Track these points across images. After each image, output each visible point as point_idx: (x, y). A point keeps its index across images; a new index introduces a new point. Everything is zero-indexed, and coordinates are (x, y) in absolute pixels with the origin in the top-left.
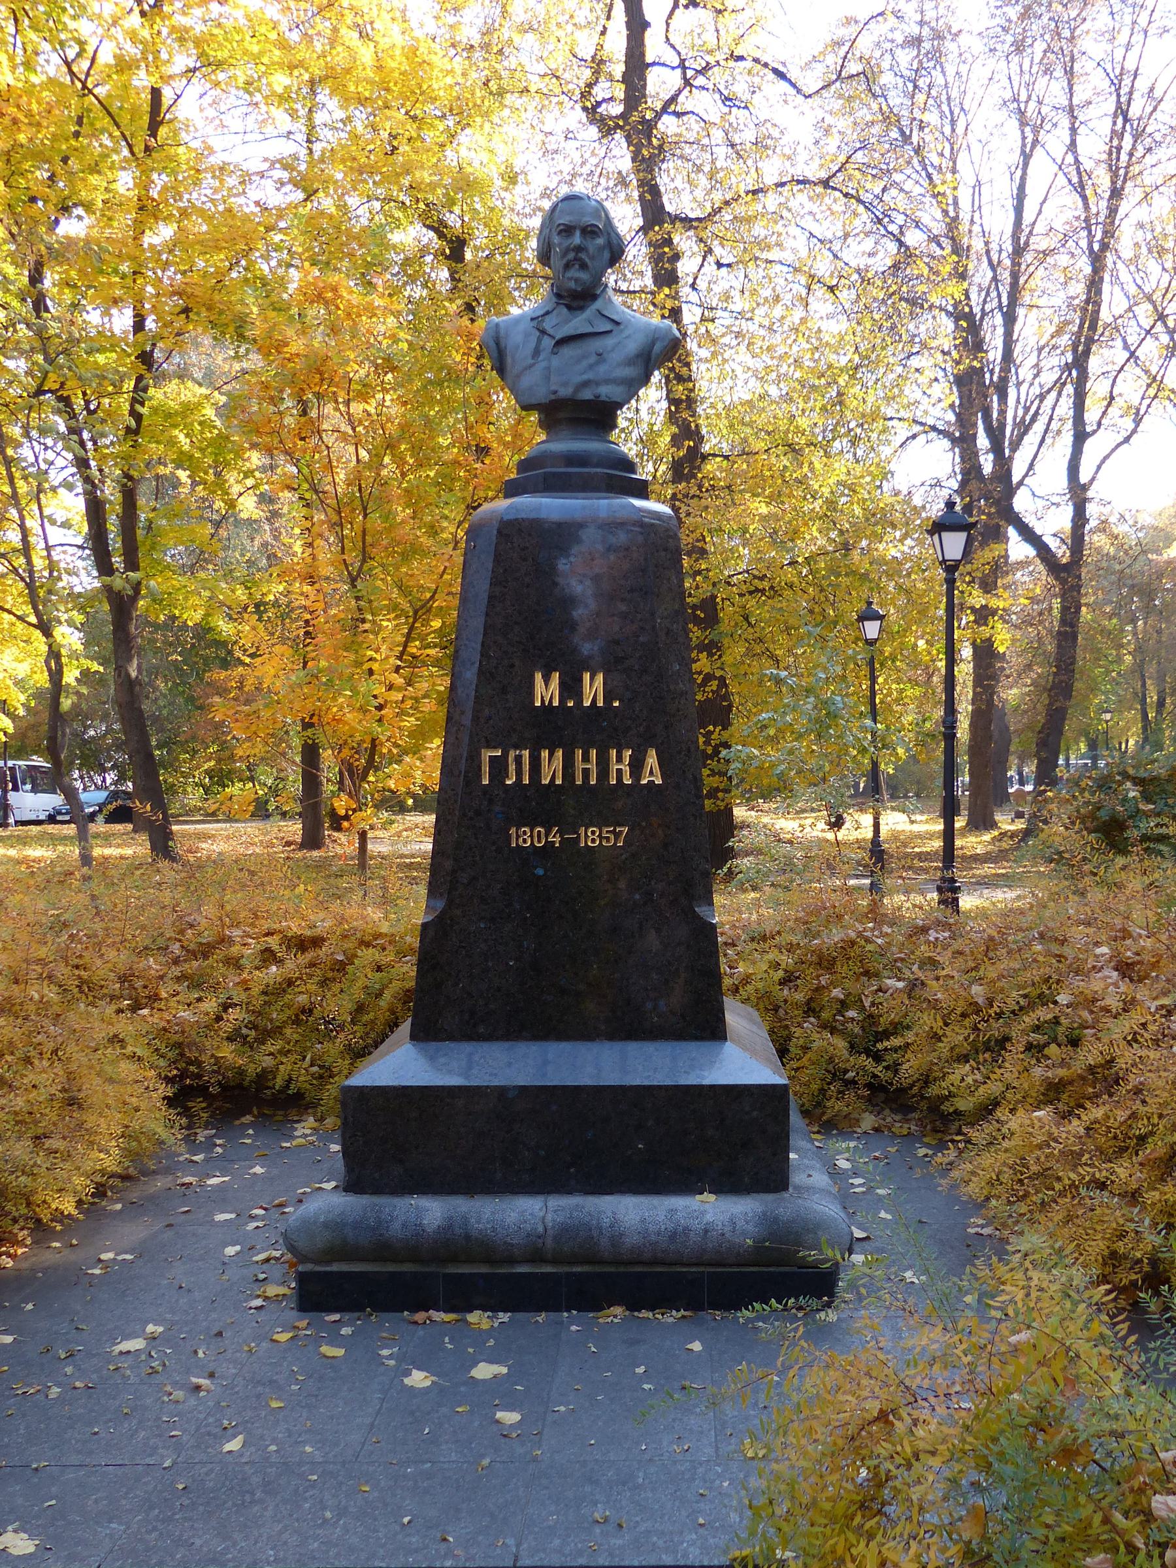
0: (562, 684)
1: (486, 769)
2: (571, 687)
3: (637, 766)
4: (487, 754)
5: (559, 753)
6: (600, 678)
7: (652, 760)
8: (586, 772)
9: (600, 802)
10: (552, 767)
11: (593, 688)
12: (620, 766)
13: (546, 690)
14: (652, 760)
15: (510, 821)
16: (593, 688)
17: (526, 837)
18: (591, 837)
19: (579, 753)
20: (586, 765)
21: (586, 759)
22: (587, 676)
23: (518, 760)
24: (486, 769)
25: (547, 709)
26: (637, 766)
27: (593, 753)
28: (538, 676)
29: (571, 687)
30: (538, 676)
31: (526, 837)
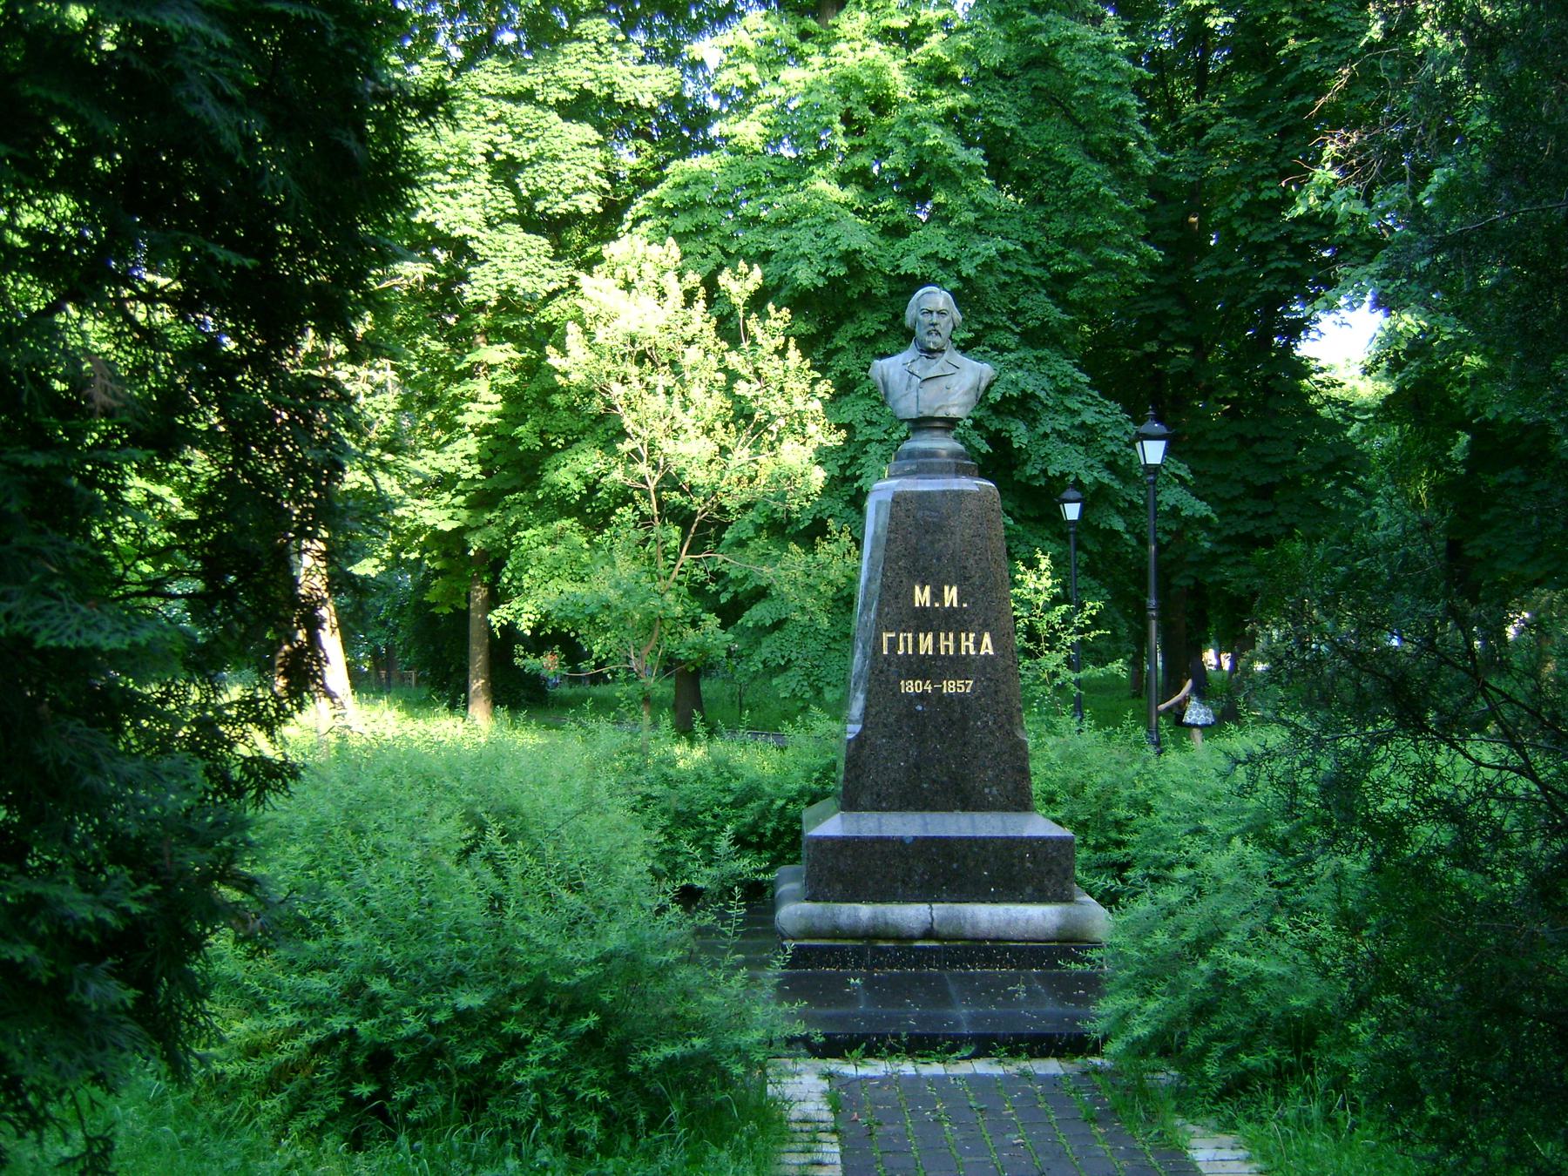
0: (932, 593)
1: (885, 645)
2: (937, 595)
3: (978, 644)
4: (886, 636)
5: (930, 636)
6: (955, 589)
7: (987, 639)
8: (947, 647)
9: (957, 665)
10: (926, 643)
11: (951, 595)
12: (968, 643)
13: (922, 597)
14: (987, 639)
15: (901, 677)
16: (951, 595)
17: (911, 687)
18: (950, 687)
19: (942, 635)
20: (947, 643)
21: (947, 639)
22: (946, 588)
23: (906, 639)
24: (885, 645)
25: (923, 609)
26: (978, 644)
27: (951, 636)
28: (917, 589)
29: (937, 595)
30: (917, 589)
31: (911, 687)
